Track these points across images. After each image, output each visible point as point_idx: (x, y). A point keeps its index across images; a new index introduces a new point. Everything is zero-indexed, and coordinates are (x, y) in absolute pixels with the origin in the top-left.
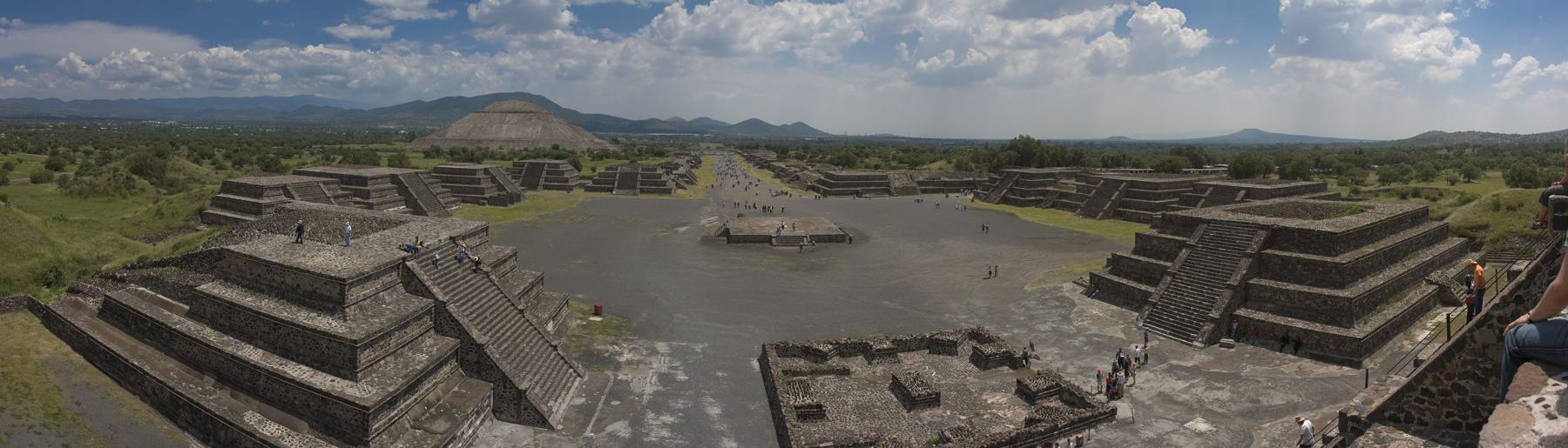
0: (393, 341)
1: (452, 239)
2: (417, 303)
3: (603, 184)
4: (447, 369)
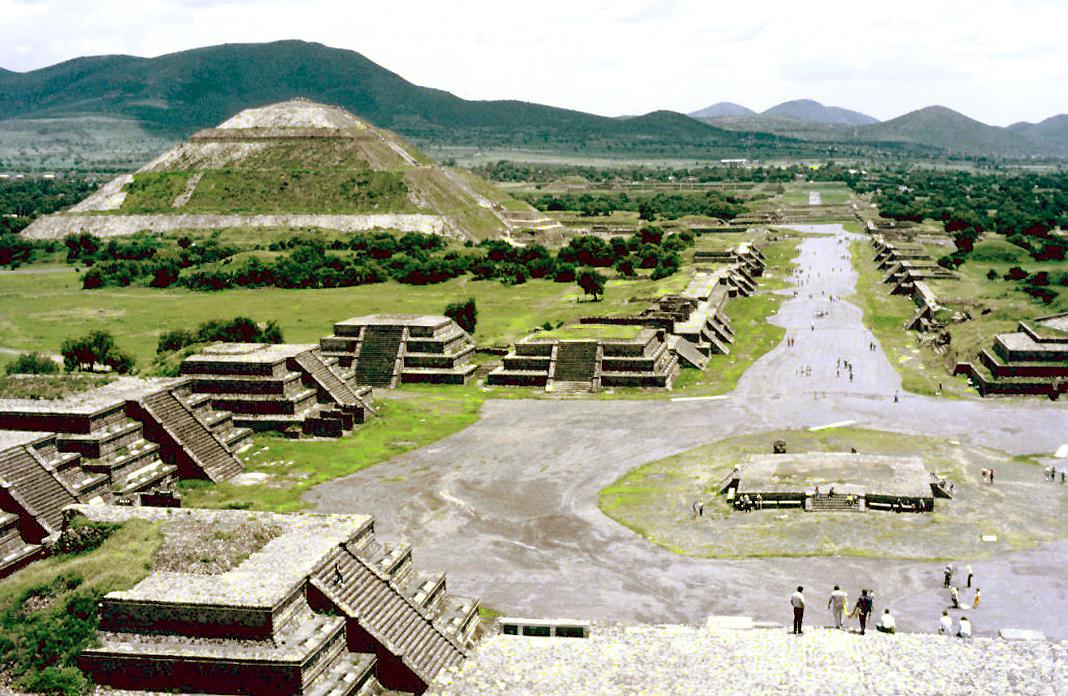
0: (321, 660)
2: (332, 625)
4: (369, 682)
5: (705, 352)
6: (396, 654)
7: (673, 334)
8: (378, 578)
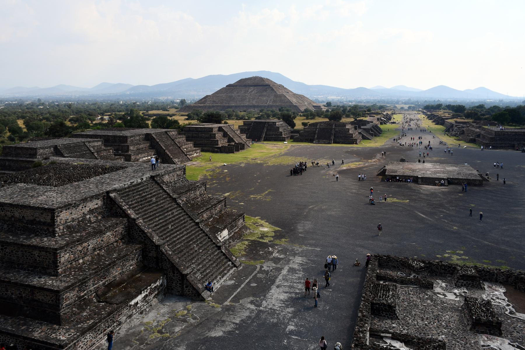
1: (152, 177)
3: (308, 136)
5: (372, 135)
6: (157, 243)
7: (360, 129)
8: (171, 197)
